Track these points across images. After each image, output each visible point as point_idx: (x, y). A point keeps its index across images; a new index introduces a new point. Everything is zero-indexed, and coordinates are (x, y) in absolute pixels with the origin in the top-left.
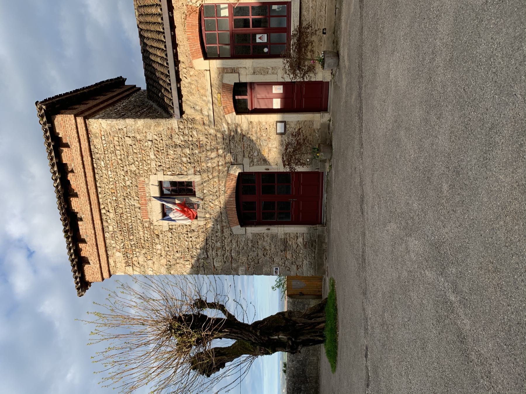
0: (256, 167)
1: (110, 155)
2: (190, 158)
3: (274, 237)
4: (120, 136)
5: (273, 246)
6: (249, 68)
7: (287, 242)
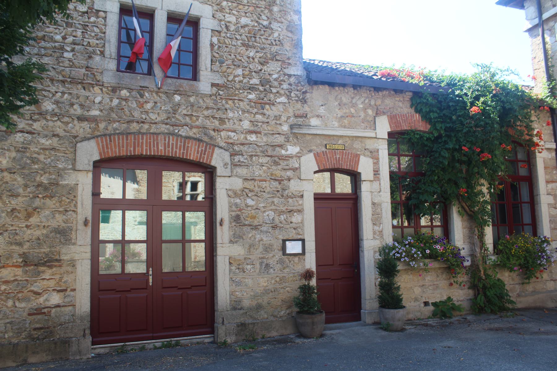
3: (64, 234)
5: (38, 233)
7: (50, 267)
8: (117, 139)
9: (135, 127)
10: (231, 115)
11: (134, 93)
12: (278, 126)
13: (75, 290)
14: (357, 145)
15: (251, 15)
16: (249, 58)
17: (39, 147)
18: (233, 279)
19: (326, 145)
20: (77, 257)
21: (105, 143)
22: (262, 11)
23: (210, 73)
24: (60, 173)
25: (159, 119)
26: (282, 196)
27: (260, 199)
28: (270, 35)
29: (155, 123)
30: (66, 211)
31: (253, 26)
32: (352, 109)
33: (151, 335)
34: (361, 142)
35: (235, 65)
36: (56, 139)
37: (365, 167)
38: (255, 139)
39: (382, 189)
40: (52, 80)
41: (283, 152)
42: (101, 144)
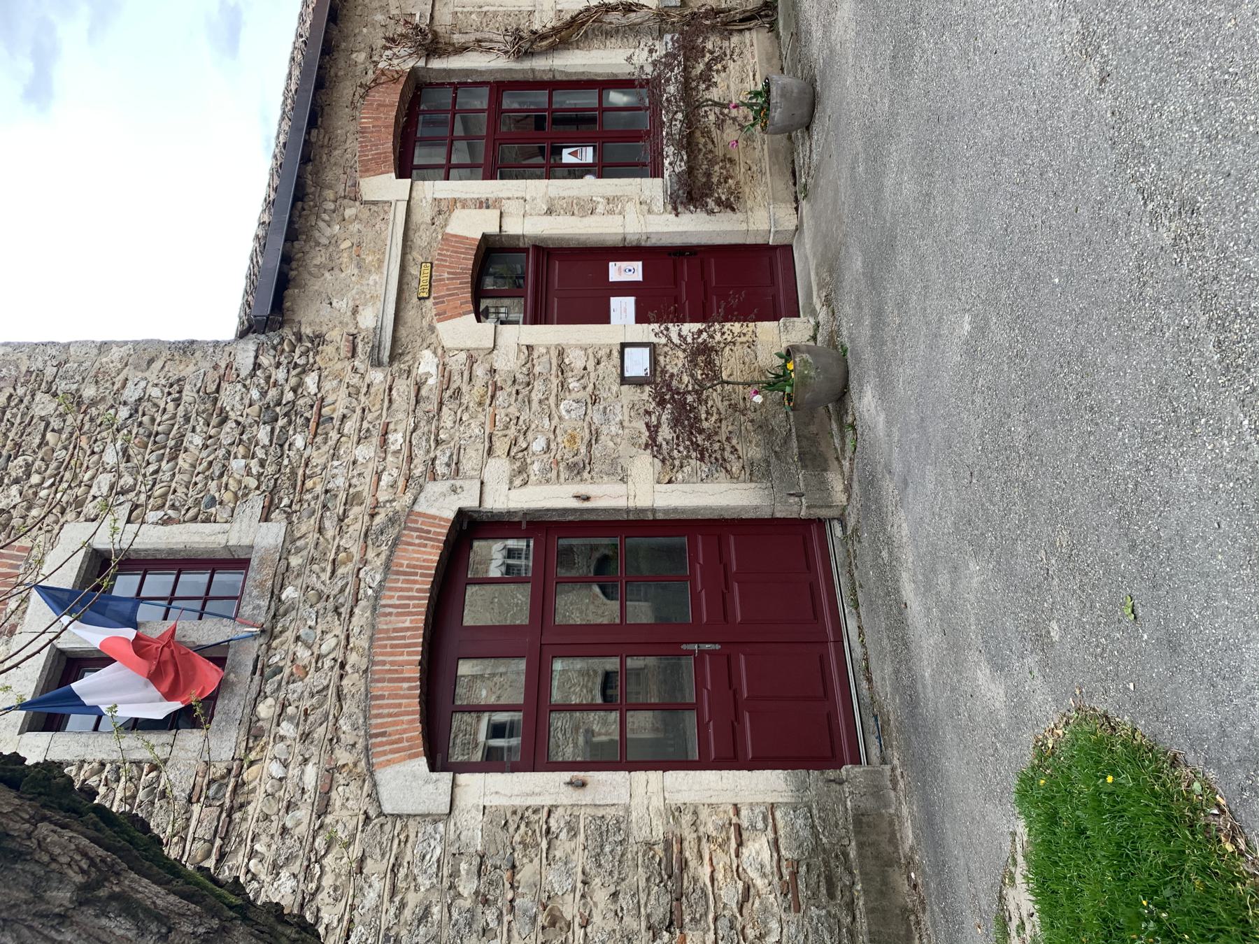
0: (538, 489)
2: (262, 464)
5: (601, 896)
7: (684, 865)
8: (379, 721)
12: (373, 390)
13: (735, 805)
15: (99, 443)
16: (206, 446)
17: (386, 904)
18: (704, 476)
19: (420, 299)
20: (657, 802)
21: (387, 748)
22: (92, 420)
23: (236, 526)
25: (338, 631)
27: (533, 426)
29: (348, 637)
30: (548, 831)
32: (343, 246)
33: (831, 646)
35: (222, 475)
36: (369, 866)
37: (472, 226)
38: (401, 434)
39: (519, 195)
41: (431, 381)
42: (390, 757)
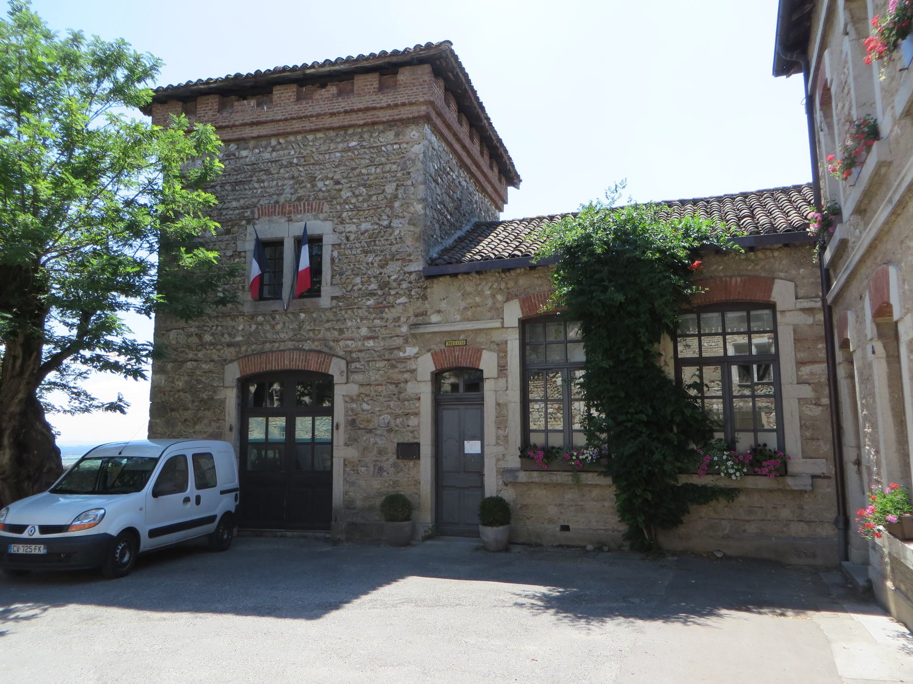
1: (367, 157)
2: (360, 289)
4: (399, 174)
6: (507, 395)
9: (268, 346)
10: (349, 324)
11: (268, 318)
12: (397, 329)
14: (481, 339)
16: (368, 264)
24: (215, 390)
25: (287, 337)
26: (399, 399)
28: (391, 235)
31: (374, 229)
34: (486, 334)
36: (212, 364)
37: (488, 363)
40: (210, 317)
